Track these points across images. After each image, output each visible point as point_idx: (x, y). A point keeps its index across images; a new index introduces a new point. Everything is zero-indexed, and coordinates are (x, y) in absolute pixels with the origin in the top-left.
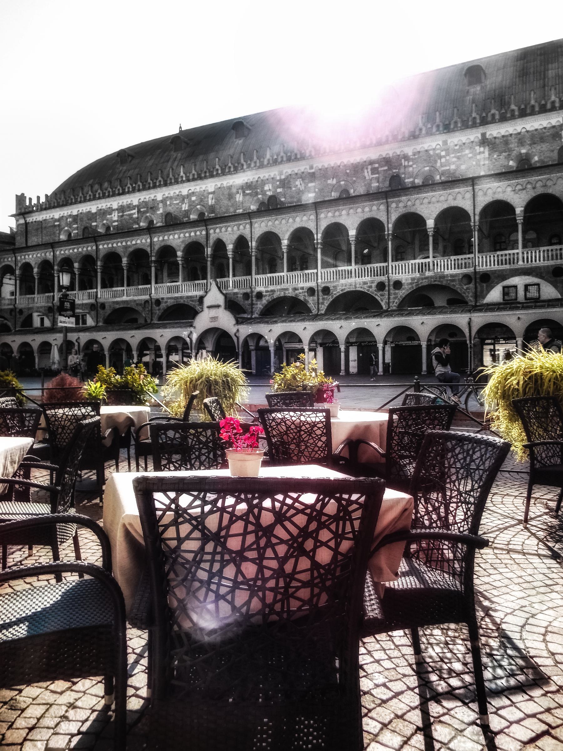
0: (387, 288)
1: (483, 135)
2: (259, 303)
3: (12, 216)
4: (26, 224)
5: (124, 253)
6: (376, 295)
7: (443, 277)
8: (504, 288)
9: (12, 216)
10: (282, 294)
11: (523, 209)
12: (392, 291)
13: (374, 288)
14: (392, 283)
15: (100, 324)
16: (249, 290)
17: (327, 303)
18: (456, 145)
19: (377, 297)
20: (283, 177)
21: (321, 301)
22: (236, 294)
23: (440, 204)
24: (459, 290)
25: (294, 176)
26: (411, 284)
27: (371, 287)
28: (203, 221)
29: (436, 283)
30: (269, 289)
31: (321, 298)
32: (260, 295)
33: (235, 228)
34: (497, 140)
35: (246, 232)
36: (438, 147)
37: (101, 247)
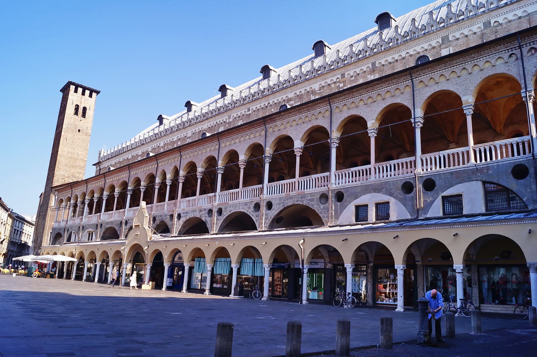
1: (374, 64)
4: (100, 169)
6: (253, 215)
7: (303, 196)
8: (357, 207)
10: (192, 216)
11: (374, 121)
13: (252, 209)
18: (352, 77)
19: (253, 218)
20: (231, 120)
22: (166, 215)
23: (305, 125)
24: (316, 210)
25: (238, 119)
26: (279, 204)
28: (158, 157)
29: (299, 203)
30: (185, 211)
33: (173, 160)
34: (385, 67)
36: (338, 80)
37: (107, 181)
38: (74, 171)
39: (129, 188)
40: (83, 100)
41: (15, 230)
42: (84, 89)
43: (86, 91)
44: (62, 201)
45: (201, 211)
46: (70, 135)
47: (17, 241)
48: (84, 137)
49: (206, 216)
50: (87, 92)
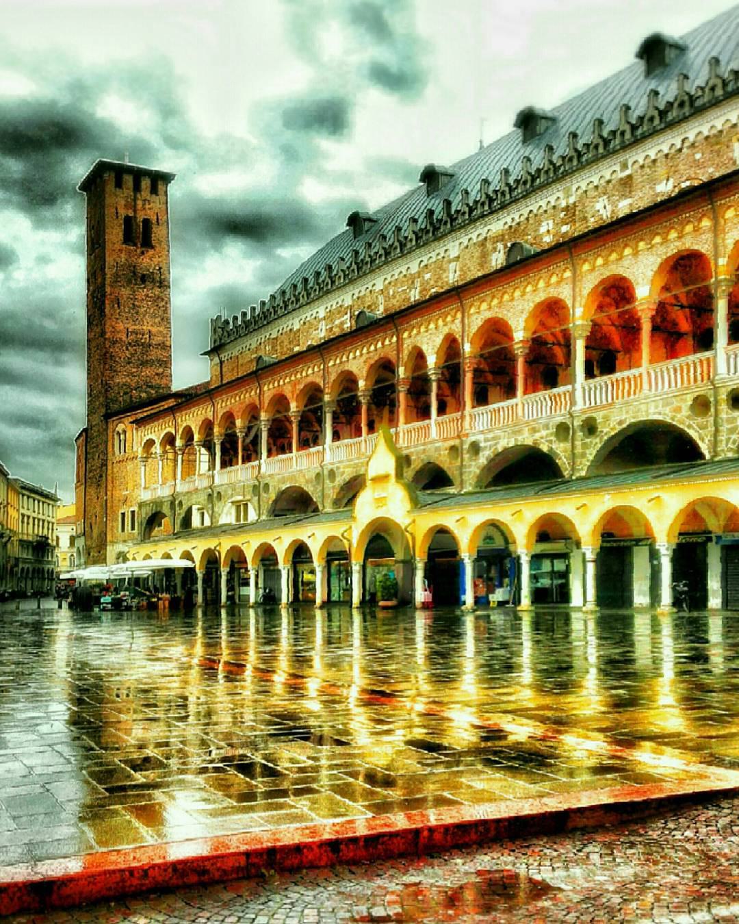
0: (712, 409)
2: (473, 463)
3: (205, 354)
4: (221, 363)
5: (293, 392)
6: (689, 426)
9: (205, 354)
12: (723, 415)
13: (685, 412)
14: (723, 396)
15: (264, 517)
16: (457, 442)
17: (591, 454)
21: (578, 450)
27: (678, 410)
31: (578, 443)
32: (475, 448)
35: (456, 328)
38: (147, 372)
39: (327, 398)
40: (140, 203)
41: (23, 515)
42: (138, 174)
43: (142, 178)
44: (150, 443)
45: (534, 430)
46: (125, 292)
47: (30, 539)
48: (157, 291)
49: (550, 442)
50: (146, 183)
